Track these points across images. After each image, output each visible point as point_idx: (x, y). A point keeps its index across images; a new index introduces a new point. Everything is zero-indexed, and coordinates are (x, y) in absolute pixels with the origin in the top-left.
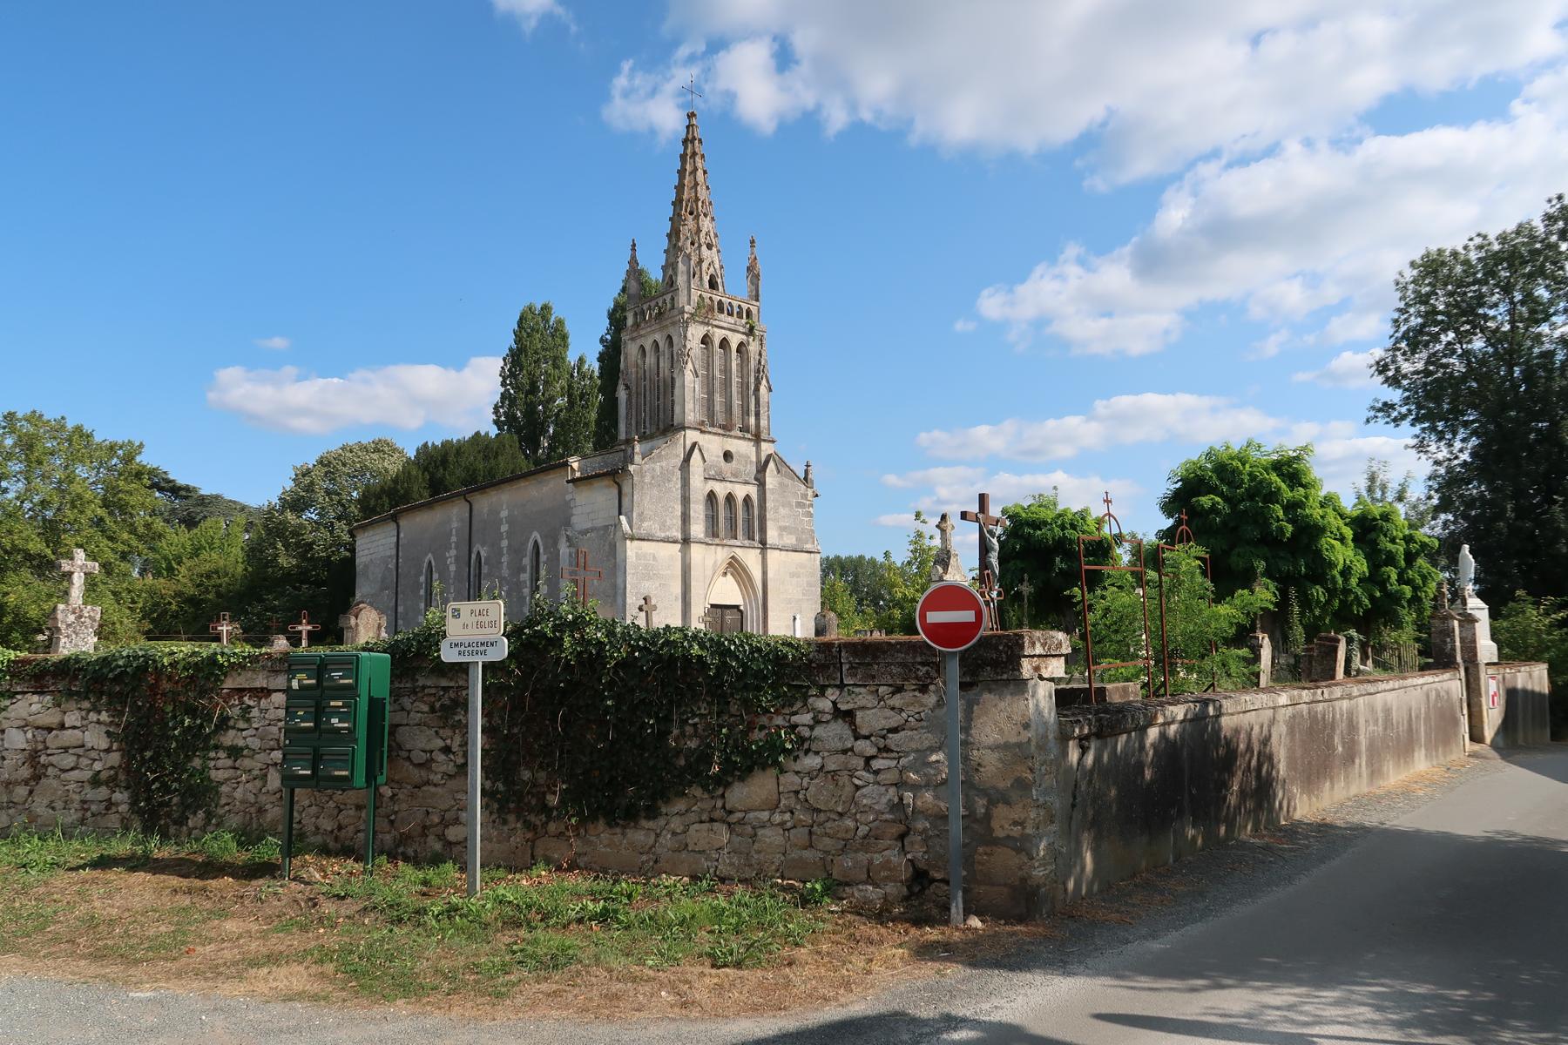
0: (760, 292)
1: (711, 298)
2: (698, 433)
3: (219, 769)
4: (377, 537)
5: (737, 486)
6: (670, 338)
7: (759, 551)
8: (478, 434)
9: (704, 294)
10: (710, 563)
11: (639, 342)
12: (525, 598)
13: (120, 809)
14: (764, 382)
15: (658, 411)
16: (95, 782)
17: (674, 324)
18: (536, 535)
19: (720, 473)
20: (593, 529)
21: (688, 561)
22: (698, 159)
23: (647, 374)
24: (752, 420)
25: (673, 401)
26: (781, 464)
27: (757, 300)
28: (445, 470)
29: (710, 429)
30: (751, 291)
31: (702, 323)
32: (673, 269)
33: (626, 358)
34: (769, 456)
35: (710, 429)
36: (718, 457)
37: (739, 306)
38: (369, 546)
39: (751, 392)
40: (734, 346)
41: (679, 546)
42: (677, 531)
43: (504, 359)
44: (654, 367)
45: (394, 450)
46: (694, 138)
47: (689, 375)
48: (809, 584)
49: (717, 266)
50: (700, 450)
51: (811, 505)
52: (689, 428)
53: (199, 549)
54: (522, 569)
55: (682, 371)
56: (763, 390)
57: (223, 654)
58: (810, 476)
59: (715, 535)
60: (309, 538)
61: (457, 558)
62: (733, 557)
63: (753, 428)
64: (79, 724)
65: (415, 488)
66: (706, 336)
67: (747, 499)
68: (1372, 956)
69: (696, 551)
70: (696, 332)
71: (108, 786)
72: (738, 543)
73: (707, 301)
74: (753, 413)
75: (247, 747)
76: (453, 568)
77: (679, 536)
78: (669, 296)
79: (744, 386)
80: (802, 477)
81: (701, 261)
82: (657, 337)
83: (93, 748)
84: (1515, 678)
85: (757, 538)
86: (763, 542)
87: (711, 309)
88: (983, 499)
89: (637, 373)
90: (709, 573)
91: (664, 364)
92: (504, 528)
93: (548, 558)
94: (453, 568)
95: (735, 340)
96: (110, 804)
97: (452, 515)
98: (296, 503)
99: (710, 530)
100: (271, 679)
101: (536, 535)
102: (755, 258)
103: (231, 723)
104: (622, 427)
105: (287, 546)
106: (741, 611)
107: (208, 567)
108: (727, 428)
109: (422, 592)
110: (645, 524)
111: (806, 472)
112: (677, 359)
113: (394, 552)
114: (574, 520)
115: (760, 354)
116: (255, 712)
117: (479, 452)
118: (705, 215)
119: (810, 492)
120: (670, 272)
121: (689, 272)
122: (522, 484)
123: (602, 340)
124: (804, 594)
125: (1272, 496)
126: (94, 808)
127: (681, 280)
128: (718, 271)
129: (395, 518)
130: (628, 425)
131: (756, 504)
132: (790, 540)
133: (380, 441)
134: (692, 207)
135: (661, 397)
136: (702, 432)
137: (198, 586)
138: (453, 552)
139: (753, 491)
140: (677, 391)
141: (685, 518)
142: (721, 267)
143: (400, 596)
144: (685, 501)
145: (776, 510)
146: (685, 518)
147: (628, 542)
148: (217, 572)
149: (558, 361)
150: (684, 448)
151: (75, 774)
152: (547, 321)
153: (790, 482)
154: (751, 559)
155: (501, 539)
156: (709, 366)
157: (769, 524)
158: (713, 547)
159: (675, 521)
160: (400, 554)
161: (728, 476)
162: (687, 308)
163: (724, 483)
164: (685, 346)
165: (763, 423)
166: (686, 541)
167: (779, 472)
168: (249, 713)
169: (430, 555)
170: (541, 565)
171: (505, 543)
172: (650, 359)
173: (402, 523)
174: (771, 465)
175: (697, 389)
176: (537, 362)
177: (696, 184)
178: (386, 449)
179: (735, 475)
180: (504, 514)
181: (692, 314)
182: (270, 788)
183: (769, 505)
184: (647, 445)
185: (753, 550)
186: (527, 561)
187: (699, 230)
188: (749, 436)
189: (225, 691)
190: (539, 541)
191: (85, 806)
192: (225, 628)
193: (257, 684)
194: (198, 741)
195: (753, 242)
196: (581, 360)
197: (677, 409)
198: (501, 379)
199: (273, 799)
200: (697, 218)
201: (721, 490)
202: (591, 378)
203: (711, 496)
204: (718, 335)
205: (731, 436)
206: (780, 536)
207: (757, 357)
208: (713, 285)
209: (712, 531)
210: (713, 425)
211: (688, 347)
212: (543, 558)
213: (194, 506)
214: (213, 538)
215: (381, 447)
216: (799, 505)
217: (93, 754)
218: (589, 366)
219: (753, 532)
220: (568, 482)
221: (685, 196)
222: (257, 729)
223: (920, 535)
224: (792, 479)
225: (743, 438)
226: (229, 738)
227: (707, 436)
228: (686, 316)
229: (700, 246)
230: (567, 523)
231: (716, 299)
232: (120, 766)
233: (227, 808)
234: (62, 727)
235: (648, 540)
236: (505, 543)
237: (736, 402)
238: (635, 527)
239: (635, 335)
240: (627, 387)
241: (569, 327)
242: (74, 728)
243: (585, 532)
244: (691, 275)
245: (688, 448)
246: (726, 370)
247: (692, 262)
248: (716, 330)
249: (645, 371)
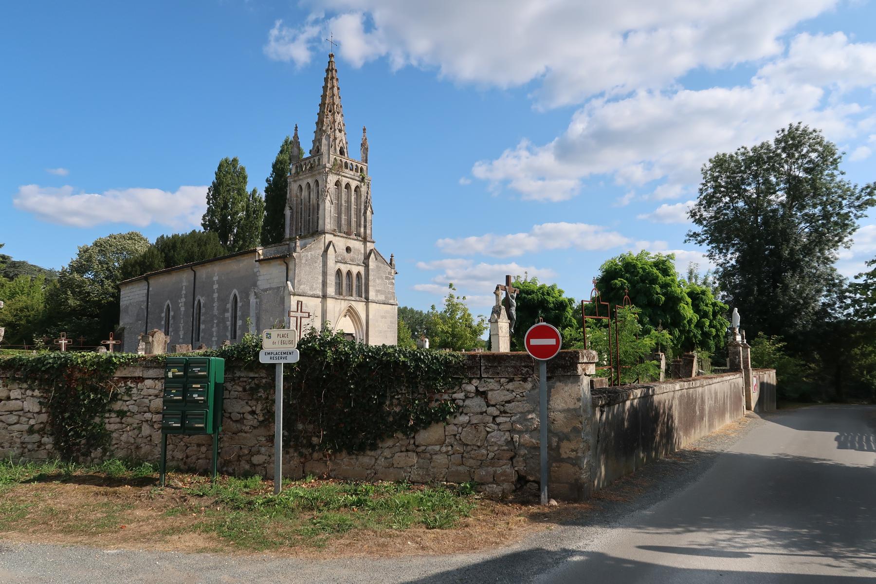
0: (368, 158)
1: (341, 160)
2: (332, 236)
3: (112, 424)
4: (134, 290)
5: (353, 267)
6: (317, 182)
8: (194, 231)
9: (337, 158)
10: (337, 309)
11: (298, 183)
12: (228, 327)
13: (47, 447)
15: (309, 223)
16: (31, 431)
17: (319, 173)
18: (235, 291)
19: (344, 259)
20: (270, 289)
21: (325, 308)
22: (335, 81)
23: (303, 201)
24: (362, 230)
25: (318, 217)
26: (377, 254)
27: (366, 163)
28: (174, 252)
29: (339, 234)
30: (363, 157)
31: (336, 174)
32: (319, 143)
33: (290, 192)
34: (371, 251)
35: (339, 234)
36: (343, 250)
37: (357, 166)
38: (129, 295)
39: (362, 214)
40: (353, 188)
41: (320, 300)
42: (319, 291)
43: (209, 189)
44: (307, 197)
45: (141, 239)
46: (333, 69)
47: (328, 203)
48: (391, 322)
49: (344, 142)
50: (334, 246)
51: (393, 279)
52: (327, 233)
53: (14, 294)
54: (226, 310)
55: (324, 200)
56: (369, 213)
57: (116, 357)
58: (393, 262)
59: (340, 293)
60: (88, 288)
61: (185, 303)
62: (350, 307)
63: (362, 234)
64: (20, 397)
65: (156, 262)
66: (338, 181)
67: (359, 274)
68: (754, 515)
69: (330, 302)
70: (332, 179)
71: (39, 434)
72: (353, 299)
73: (339, 162)
74: (363, 226)
75: (129, 411)
76: (183, 309)
77: (320, 294)
78: (317, 157)
79: (358, 211)
80: (389, 262)
81: (335, 139)
82: (310, 180)
83: (29, 411)
84: (763, 377)
85: (363, 296)
86: (367, 298)
87: (341, 166)
88: (508, 278)
89: (297, 200)
90: (337, 315)
91: (313, 196)
92: (216, 286)
93: (242, 305)
94: (183, 309)
95: (354, 184)
96: (40, 444)
97: (183, 279)
98: (80, 267)
99: (338, 291)
100: (145, 372)
101: (235, 291)
102: (366, 139)
103: (119, 397)
104: (287, 231)
105: (73, 293)
106: (354, 337)
107: (21, 304)
108: (348, 233)
109: (163, 323)
110: (302, 287)
111: (391, 260)
112: (320, 194)
113: (145, 299)
114: (259, 283)
115: (367, 193)
116: (134, 391)
117: (195, 242)
118: (338, 113)
119: (393, 271)
120: (317, 144)
121: (329, 144)
122: (228, 261)
123: (267, 180)
124: (388, 328)
125: (654, 280)
126: (30, 446)
127: (324, 149)
128: (345, 145)
129: (146, 279)
130: (291, 230)
131: (363, 277)
132: (381, 298)
133: (132, 233)
134: (331, 108)
135: (311, 214)
136: (335, 235)
137: (15, 316)
138: (183, 300)
139: (362, 269)
140: (321, 212)
141: (324, 284)
142: (347, 143)
143: (149, 325)
144: (325, 274)
145: (374, 281)
146: (324, 284)
147: (292, 296)
148: (27, 308)
149: (240, 191)
150: (325, 244)
151: (17, 427)
152: (235, 168)
153: (382, 265)
154: (360, 307)
155: (214, 292)
156: (339, 198)
157: (371, 288)
158: (339, 301)
160: (149, 300)
161: (348, 261)
162: (328, 165)
164: (326, 186)
165: (368, 232)
166: (324, 297)
167: (376, 259)
168: (131, 391)
169: (168, 301)
170: (238, 308)
171: (216, 295)
172: (305, 193)
173: (152, 281)
174: (372, 255)
175: (332, 211)
176: (228, 191)
177: (333, 95)
178: (136, 238)
179: (352, 260)
180: (216, 278)
181: (330, 169)
182: (143, 434)
183: (371, 278)
184: (303, 242)
186: (229, 306)
187: (334, 121)
188: (360, 239)
189: (115, 378)
190: (237, 294)
191: (24, 446)
192: (63, 342)
193: (136, 375)
194: (99, 407)
195: (364, 130)
196: (254, 191)
197: (321, 222)
198: (207, 200)
199: (145, 441)
200: (333, 114)
201: (345, 268)
202: (260, 201)
203: (339, 272)
204: (344, 181)
205: (350, 239)
206: (377, 295)
207: (366, 195)
208: (342, 152)
209: (339, 292)
210: (340, 232)
211: (328, 187)
212: (239, 304)
213: (9, 267)
214: (23, 288)
215: (132, 237)
216: (387, 278)
217: (29, 415)
218: (259, 195)
219: (362, 293)
220: (256, 261)
221: (327, 102)
222: (135, 401)
223: (451, 296)
224: (383, 264)
225: (357, 240)
226: (118, 406)
227: (337, 238)
228: (327, 169)
229: (335, 130)
230: (255, 285)
231: (344, 160)
232: (47, 422)
233: (116, 446)
234: (8, 398)
235: (303, 296)
236: (216, 295)
237: (354, 219)
239: (296, 178)
240: (291, 208)
241: (248, 172)
242: (17, 399)
243: (266, 290)
244: (329, 146)
245: (326, 244)
246: (348, 201)
247: (331, 139)
248: (343, 178)
249: (301, 200)
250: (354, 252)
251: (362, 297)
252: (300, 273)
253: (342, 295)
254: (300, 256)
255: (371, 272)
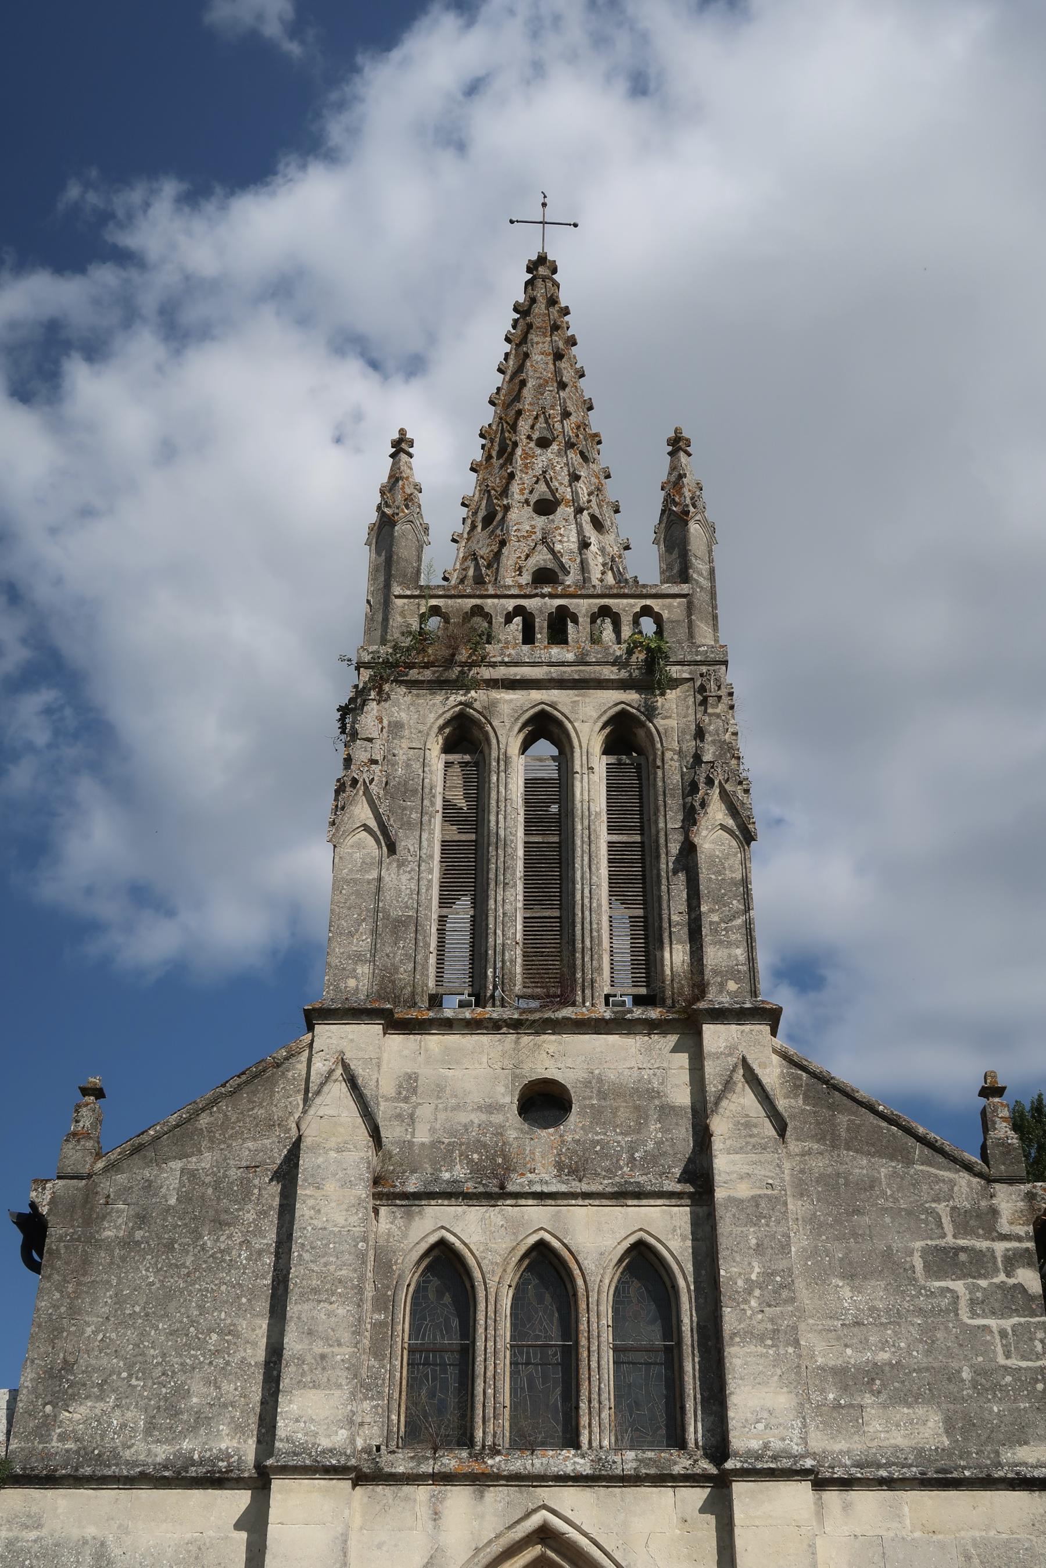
1: (477, 610)
7: (699, 1495)
14: (716, 813)
30: (670, 567)
31: (440, 685)
36: (491, 1108)
42: (238, 1429)
85: (695, 1431)
131: (685, 1284)
153: (884, 1168)
158: (422, 1493)
159: (229, 1388)
163: (509, 1210)
185: (663, 1498)
227: (434, 1042)
235: (77, 1481)
238: (26, 1424)
250: (596, 1114)
251: (681, 1444)
252: (74, 1312)
253: (465, 1439)
254: (89, 1194)
255: (727, 1228)
